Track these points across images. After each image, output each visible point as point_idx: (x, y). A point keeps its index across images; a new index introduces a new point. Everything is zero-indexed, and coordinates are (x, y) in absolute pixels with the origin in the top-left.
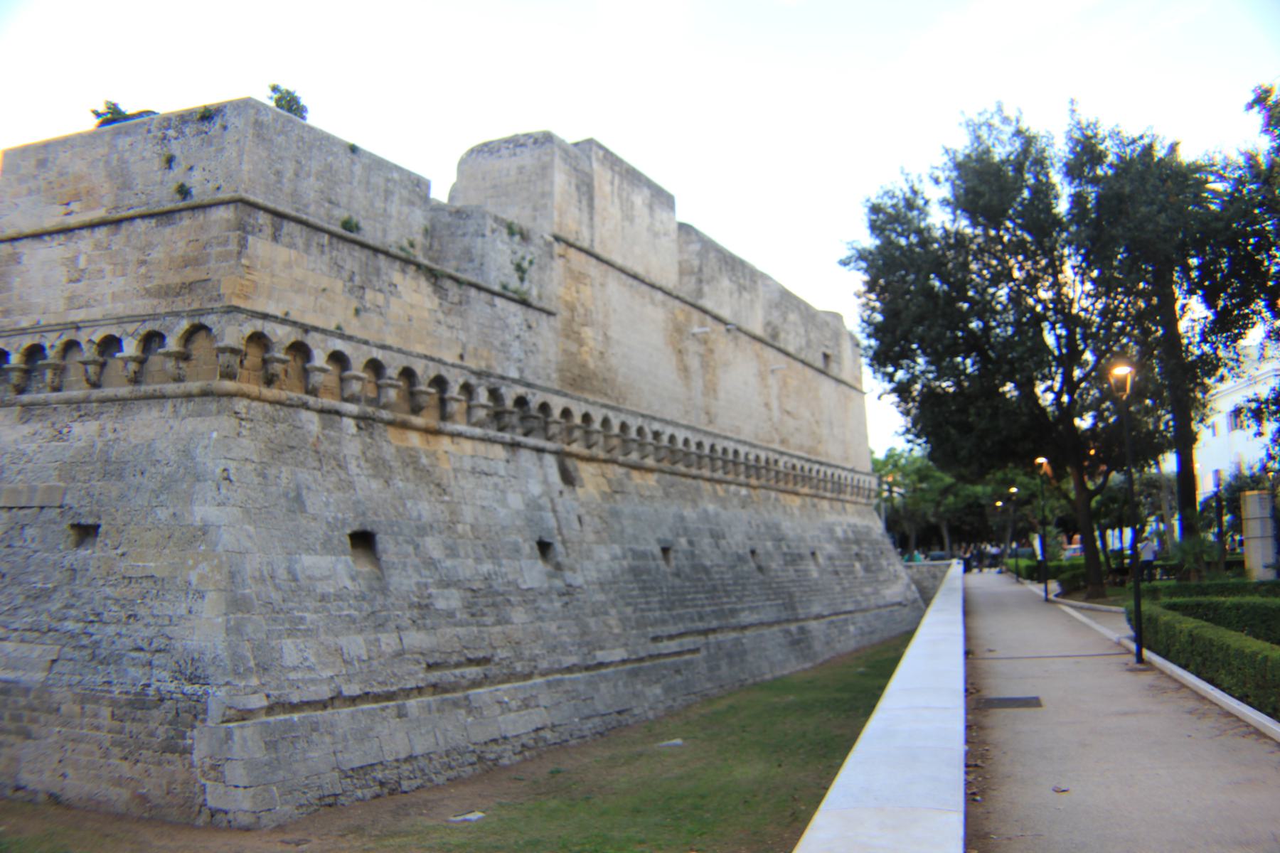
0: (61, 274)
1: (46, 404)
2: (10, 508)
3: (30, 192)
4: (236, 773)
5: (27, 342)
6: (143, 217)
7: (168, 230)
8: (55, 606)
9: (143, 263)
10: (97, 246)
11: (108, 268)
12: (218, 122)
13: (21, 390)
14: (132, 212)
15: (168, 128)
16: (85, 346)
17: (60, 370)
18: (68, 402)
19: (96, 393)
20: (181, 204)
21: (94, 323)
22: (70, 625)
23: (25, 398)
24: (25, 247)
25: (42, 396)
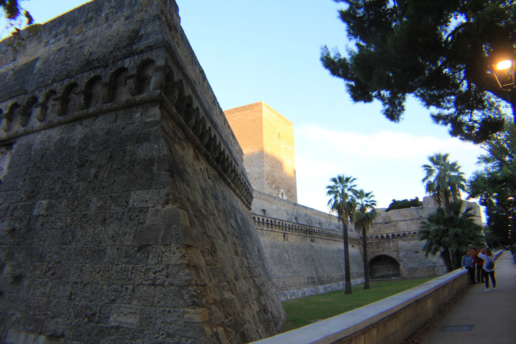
4: (440, 271)
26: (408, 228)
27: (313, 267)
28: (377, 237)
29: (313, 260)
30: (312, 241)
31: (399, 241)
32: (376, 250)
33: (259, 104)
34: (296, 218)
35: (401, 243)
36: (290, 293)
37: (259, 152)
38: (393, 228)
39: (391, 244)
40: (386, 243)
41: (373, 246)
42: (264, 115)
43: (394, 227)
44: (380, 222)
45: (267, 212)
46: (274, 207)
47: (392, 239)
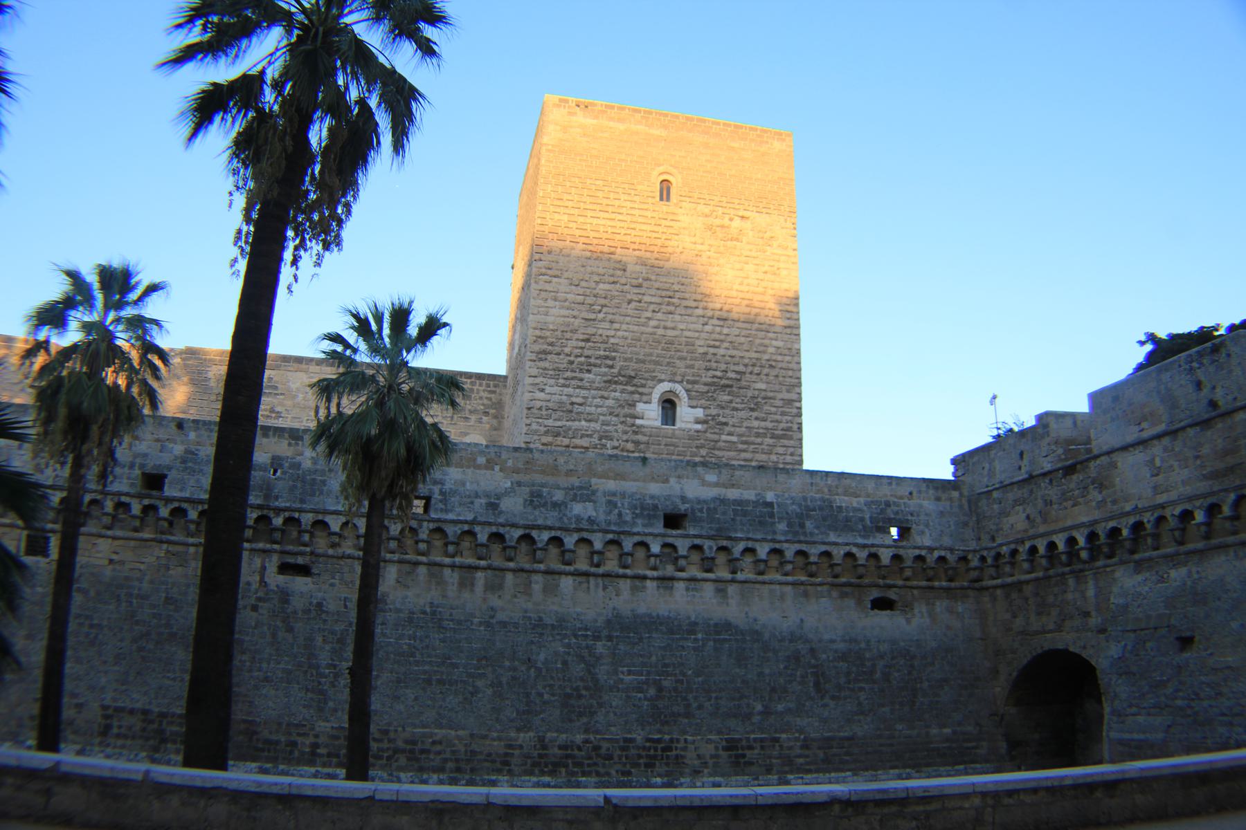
0: (1146, 472)
1: (1150, 559)
2: (1135, 631)
3: (1113, 420)
5: (1132, 520)
6: (1190, 426)
7: (1209, 433)
8: (1169, 691)
9: (1197, 457)
10: (1165, 450)
11: (1176, 464)
12: (1224, 351)
13: (1132, 552)
14: (1182, 424)
15: (1192, 362)
16: (1170, 519)
17: (1156, 536)
18: (1165, 556)
19: (1183, 549)
20: (1213, 414)
21: (1173, 503)
22: (1179, 702)
23: (1137, 557)
24: (1118, 457)
25: (1147, 554)
26: (1156, 489)
35: (1127, 583)
38: (1095, 495)
40: (1071, 582)
44: (1048, 467)
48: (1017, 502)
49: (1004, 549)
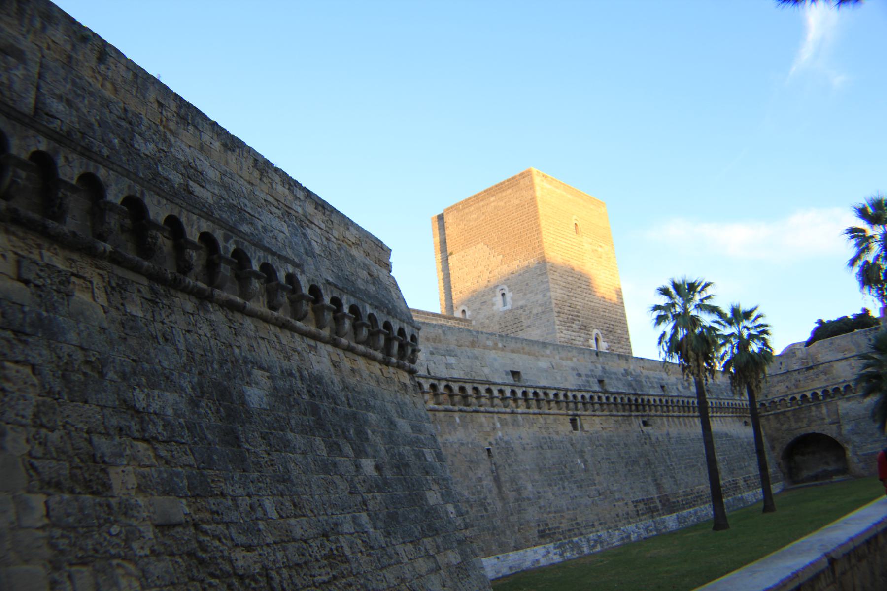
0: (848, 368)
5: (845, 384)
27: (650, 479)
28: (793, 399)
29: (649, 463)
30: (645, 424)
31: (840, 403)
32: (794, 425)
33: (526, 175)
34: (601, 382)
36: (588, 540)
37: (539, 263)
38: (823, 377)
39: (824, 410)
40: (813, 408)
41: (788, 418)
42: (538, 193)
43: (826, 374)
44: (796, 368)
45: (524, 376)
46: (543, 364)
47: (824, 399)
48: (778, 382)
49: (776, 400)
